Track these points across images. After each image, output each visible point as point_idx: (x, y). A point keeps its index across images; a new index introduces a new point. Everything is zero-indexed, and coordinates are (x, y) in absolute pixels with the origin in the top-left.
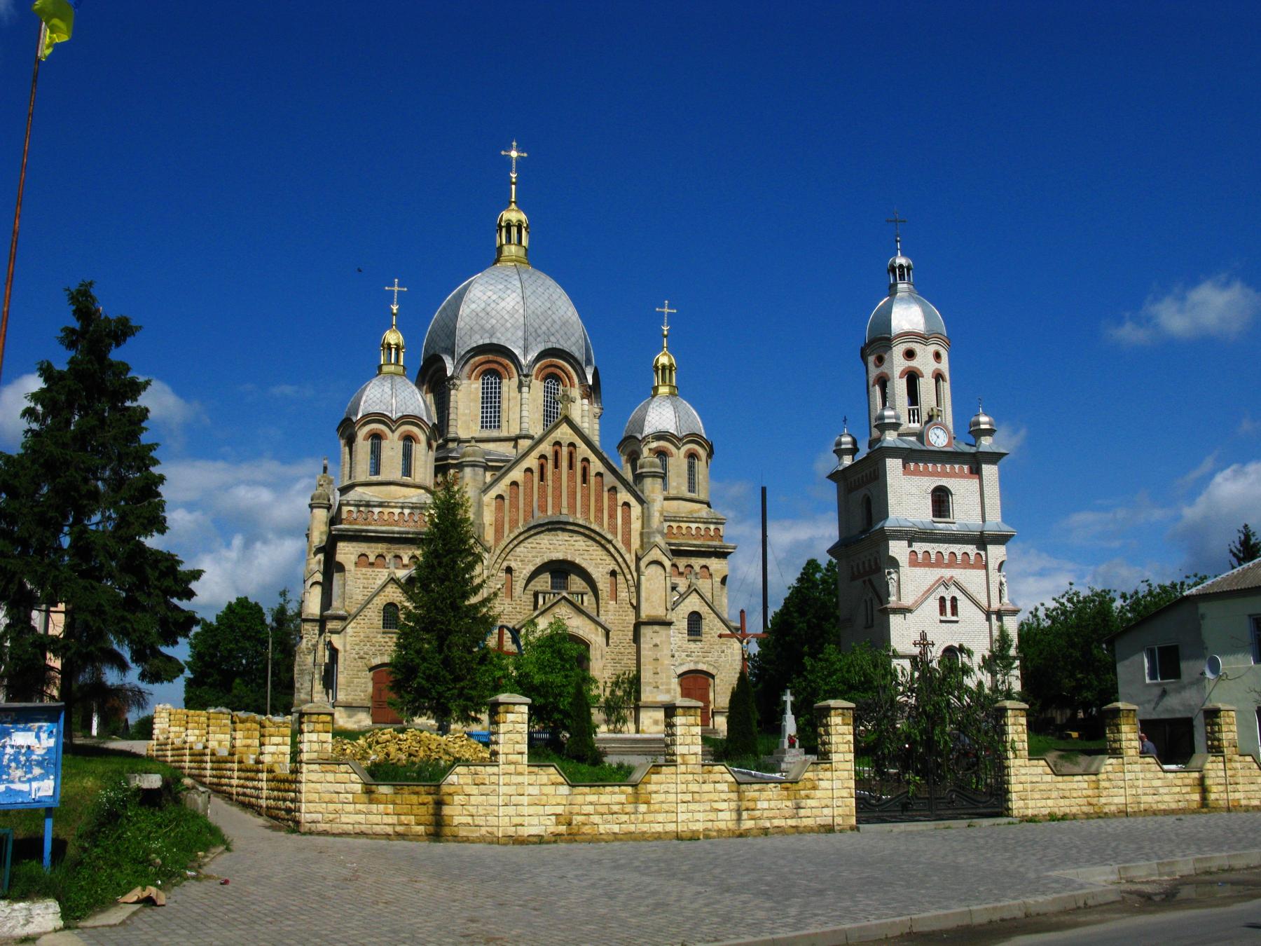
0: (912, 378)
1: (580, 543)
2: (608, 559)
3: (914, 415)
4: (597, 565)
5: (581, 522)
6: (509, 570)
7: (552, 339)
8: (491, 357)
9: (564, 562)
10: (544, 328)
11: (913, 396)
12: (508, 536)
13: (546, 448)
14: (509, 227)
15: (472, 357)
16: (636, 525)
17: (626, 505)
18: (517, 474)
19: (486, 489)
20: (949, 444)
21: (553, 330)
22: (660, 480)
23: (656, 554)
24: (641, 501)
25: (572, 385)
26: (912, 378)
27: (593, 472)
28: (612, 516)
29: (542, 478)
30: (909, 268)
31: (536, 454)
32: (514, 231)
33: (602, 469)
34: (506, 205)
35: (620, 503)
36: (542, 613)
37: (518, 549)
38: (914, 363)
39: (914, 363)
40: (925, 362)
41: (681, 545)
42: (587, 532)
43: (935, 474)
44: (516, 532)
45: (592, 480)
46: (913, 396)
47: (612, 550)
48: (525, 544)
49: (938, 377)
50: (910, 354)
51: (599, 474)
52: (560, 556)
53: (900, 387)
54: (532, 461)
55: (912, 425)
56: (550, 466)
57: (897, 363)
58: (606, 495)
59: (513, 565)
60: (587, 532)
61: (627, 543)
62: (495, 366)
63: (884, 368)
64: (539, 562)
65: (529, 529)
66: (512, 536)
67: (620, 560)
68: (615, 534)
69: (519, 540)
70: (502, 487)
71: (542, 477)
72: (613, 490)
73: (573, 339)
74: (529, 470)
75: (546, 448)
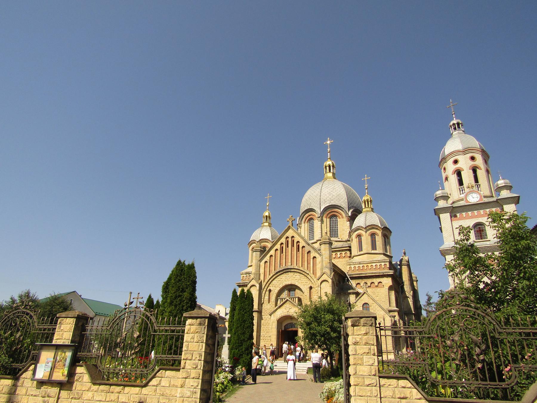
0: (459, 173)
1: (297, 276)
2: (309, 282)
3: (461, 191)
4: (304, 285)
5: (296, 268)
6: (270, 291)
7: (332, 202)
8: (310, 213)
9: (291, 285)
10: (328, 199)
11: (461, 183)
12: (268, 277)
13: (283, 240)
14: (326, 167)
15: (304, 215)
16: (318, 266)
17: (314, 257)
18: (272, 252)
19: (260, 261)
20: (481, 199)
21: (332, 199)
22: (328, 245)
23: (325, 277)
24: (320, 255)
25: (343, 218)
26: (459, 173)
27: (301, 247)
28: (308, 263)
29: (282, 252)
30: (458, 124)
31: (279, 243)
32: (328, 168)
33: (304, 244)
34: (326, 160)
35: (312, 257)
36: (280, 307)
37: (273, 282)
38: (458, 166)
39: (458, 166)
40: (465, 163)
41: (366, 273)
42: (299, 271)
43: (473, 217)
44: (272, 275)
45: (300, 249)
46: (461, 183)
47: (310, 278)
48: (276, 279)
49: (474, 170)
50: (456, 162)
51: (303, 247)
52: (289, 283)
53: (453, 179)
54: (278, 246)
55: (461, 196)
56: (284, 246)
57: (450, 167)
58: (306, 254)
59: (271, 288)
60: (299, 271)
61: (314, 273)
62: (311, 217)
63: (446, 173)
64: (281, 286)
65: (277, 273)
66: (270, 277)
67: (313, 281)
68: (310, 271)
69: (273, 278)
70: (267, 258)
71: (282, 252)
72: (309, 252)
73: (342, 200)
74: (277, 250)
75: (283, 240)
